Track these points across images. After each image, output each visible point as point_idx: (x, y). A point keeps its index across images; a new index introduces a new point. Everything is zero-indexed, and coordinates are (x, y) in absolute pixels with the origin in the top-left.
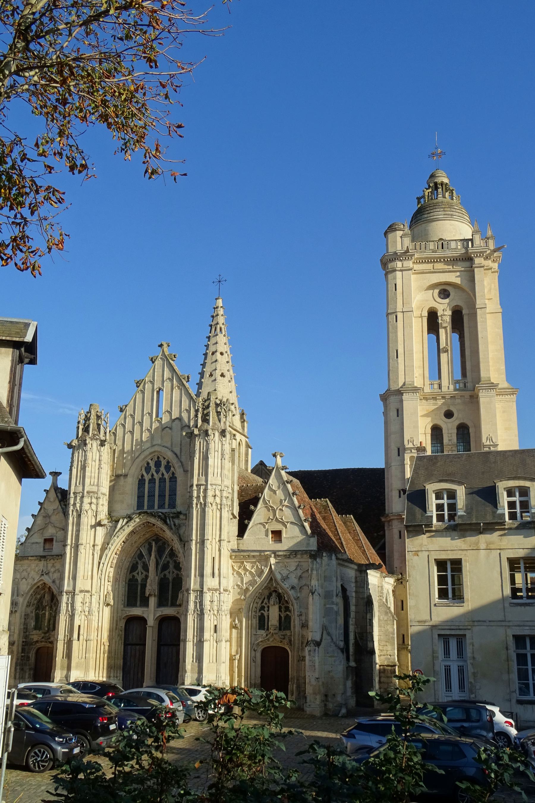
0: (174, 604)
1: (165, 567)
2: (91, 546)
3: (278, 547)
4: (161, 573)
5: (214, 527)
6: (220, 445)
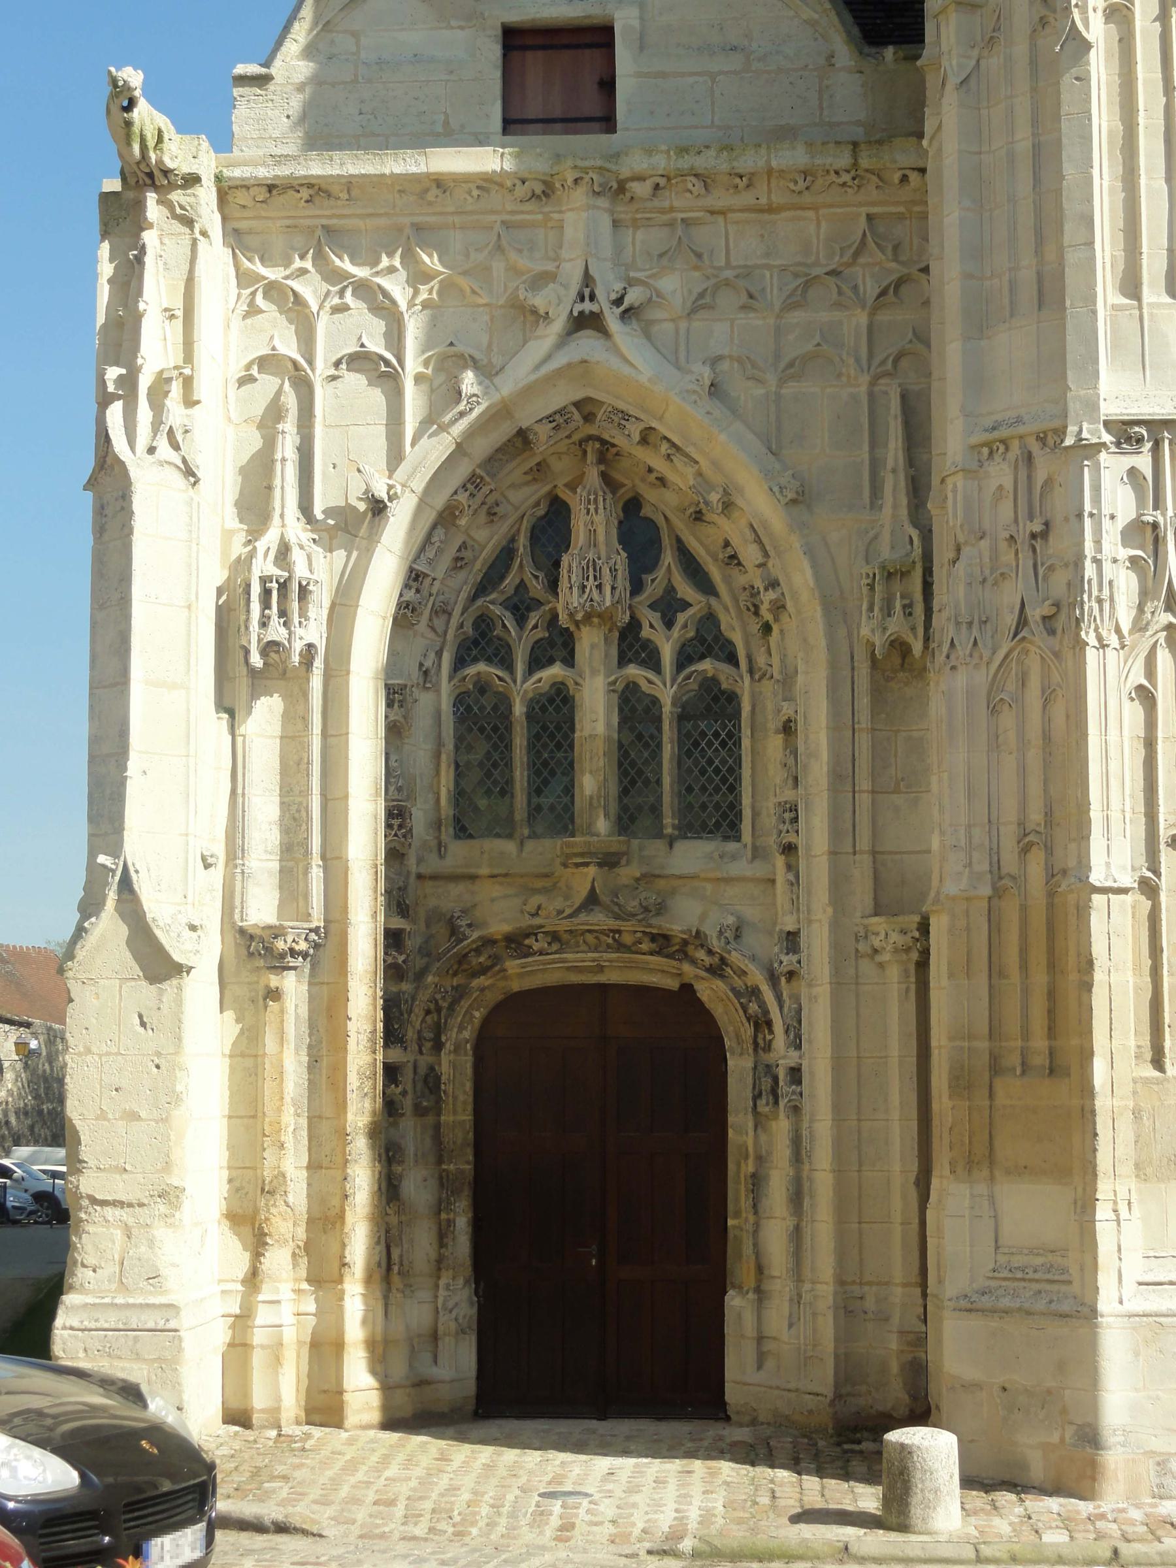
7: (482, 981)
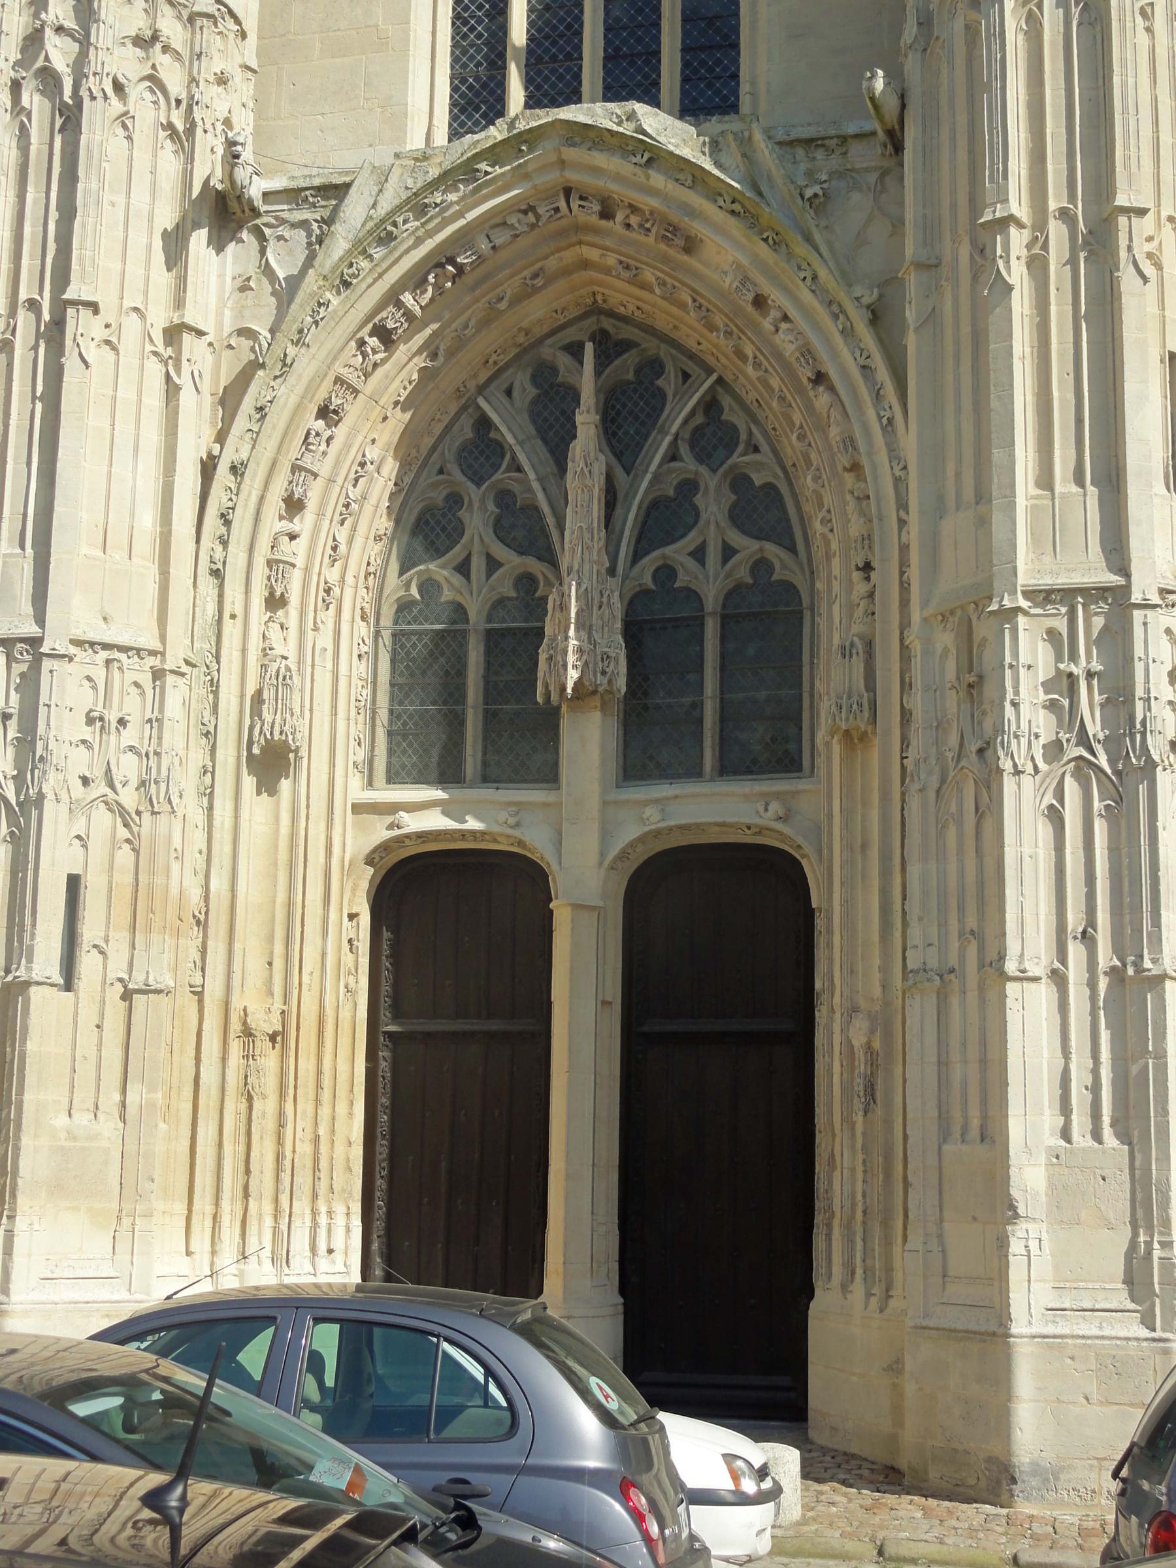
4: (636, 557)
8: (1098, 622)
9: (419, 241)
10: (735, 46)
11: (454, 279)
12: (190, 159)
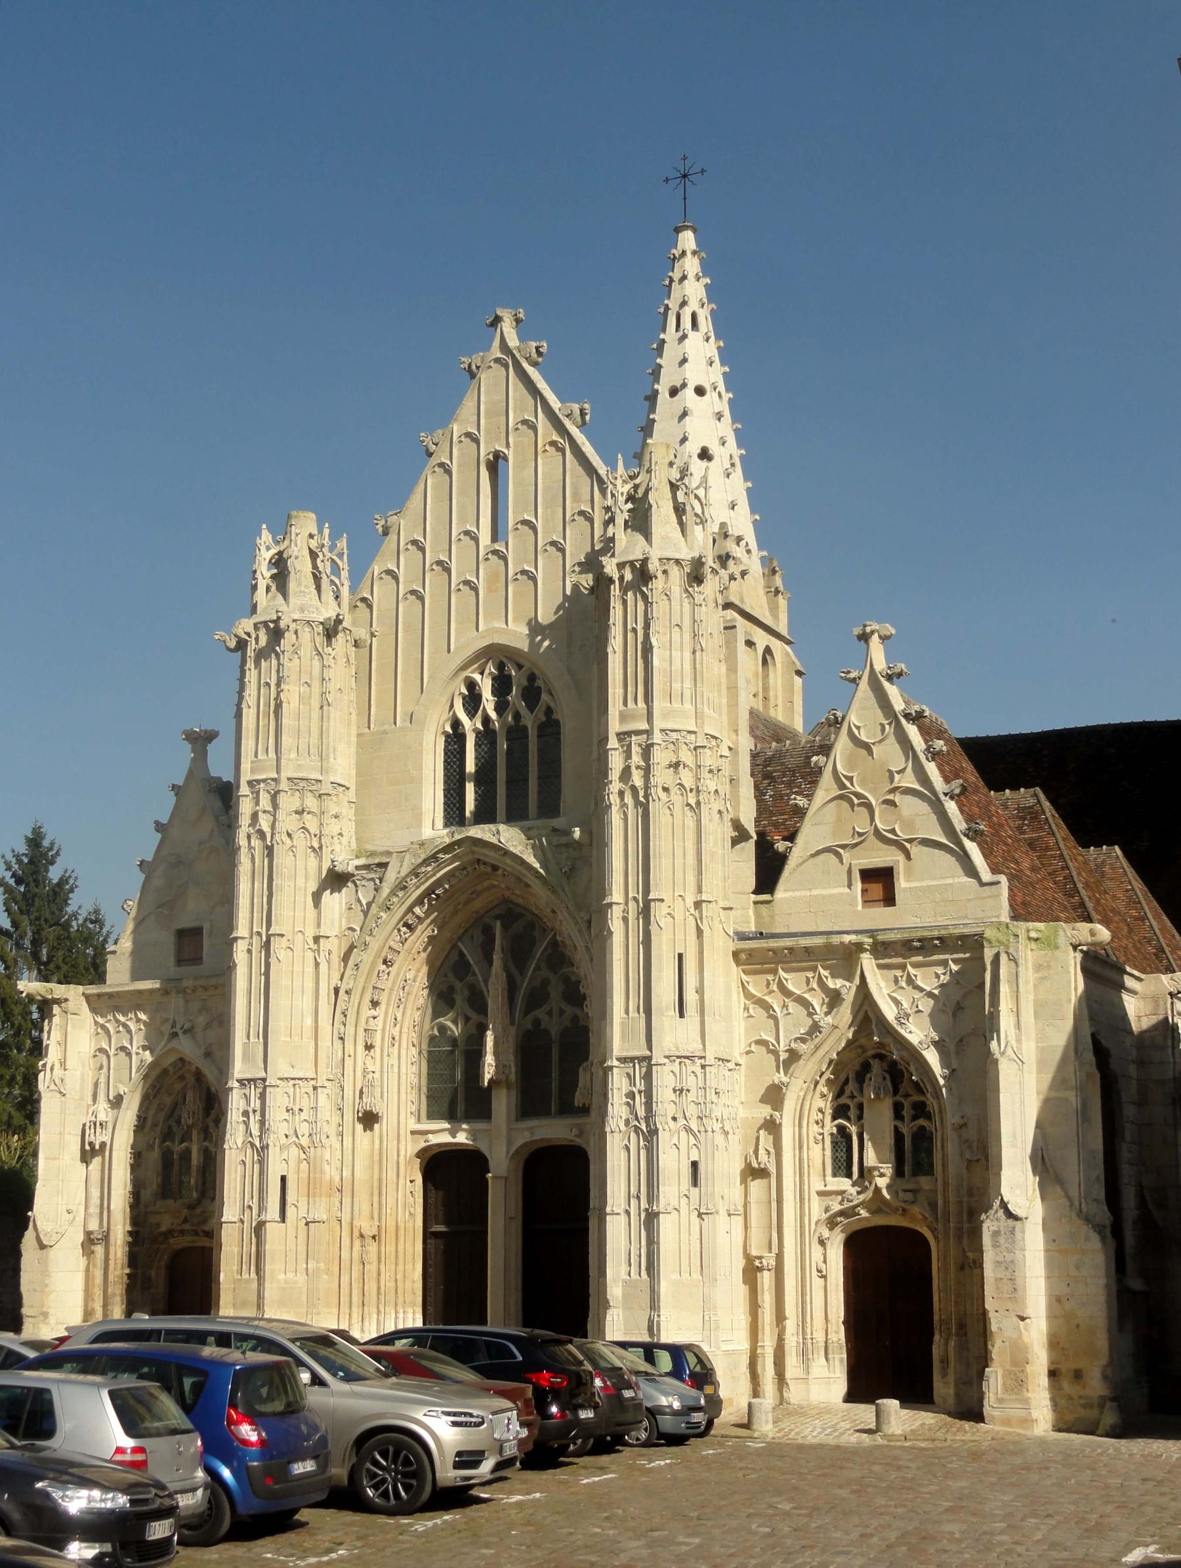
0: (568, 1108)
1: (537, 998)
2: (311, 941)
3: (881, 918)
4: (525, 1015)
5: (679, 861)
6: (687, 607)
7: (162, 1247)
8: (644, 1070)
9: (417, 888)
10: (559, 776)
11: (436, 900)
12: (321, 861)
